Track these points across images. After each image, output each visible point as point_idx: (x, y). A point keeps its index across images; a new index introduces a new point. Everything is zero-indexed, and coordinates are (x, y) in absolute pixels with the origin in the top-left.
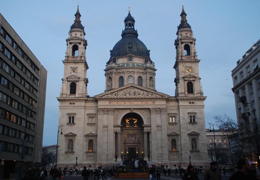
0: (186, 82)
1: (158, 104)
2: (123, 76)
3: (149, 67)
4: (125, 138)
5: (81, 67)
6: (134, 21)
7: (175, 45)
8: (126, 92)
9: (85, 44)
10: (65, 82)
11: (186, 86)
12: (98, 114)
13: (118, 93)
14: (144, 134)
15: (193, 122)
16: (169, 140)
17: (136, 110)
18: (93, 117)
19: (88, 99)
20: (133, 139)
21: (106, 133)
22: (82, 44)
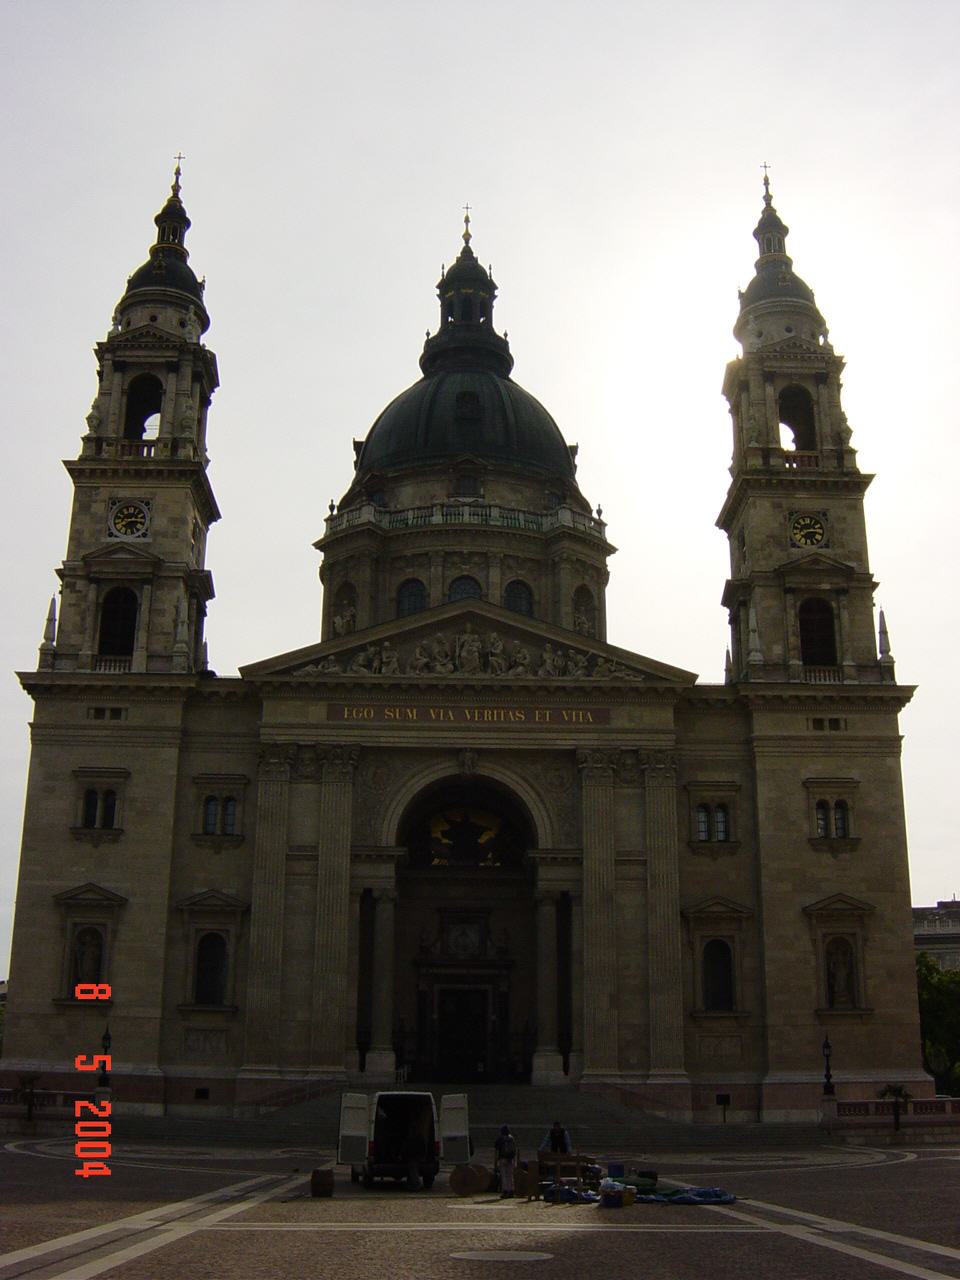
1: (627, 725)
2: (423, 577)
3: (574, 529)
8: (436, 649)
13: (384, 655)
18: (229, 799)
22: (187, 371)
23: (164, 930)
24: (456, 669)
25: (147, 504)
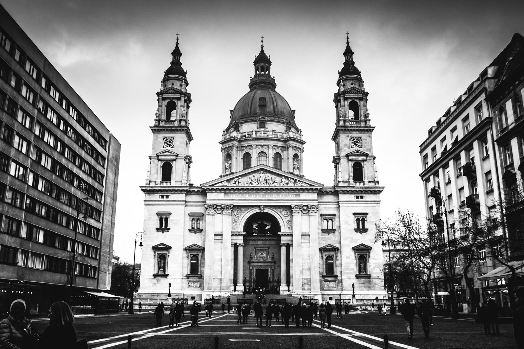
0: (351, 164)
2: (250, 151)
4: (251, 253)
5: (180, 138)
6: (269, 63)
7: (334, 101)
8: (253, 178)
9: (188, 100)
10: (154, 162)
11: (351, 169)
12: (207, 213)
13: (239, 180)
14: (281, 246)
15: (361, 228)
16: (322, 257)
17: (269, 207)
18: (198, 220)
19: (191, 190)
20: (264, 255)
21: (220, 244)
23: (182, 255)
24: (258, 184)
25: (173, 138)
